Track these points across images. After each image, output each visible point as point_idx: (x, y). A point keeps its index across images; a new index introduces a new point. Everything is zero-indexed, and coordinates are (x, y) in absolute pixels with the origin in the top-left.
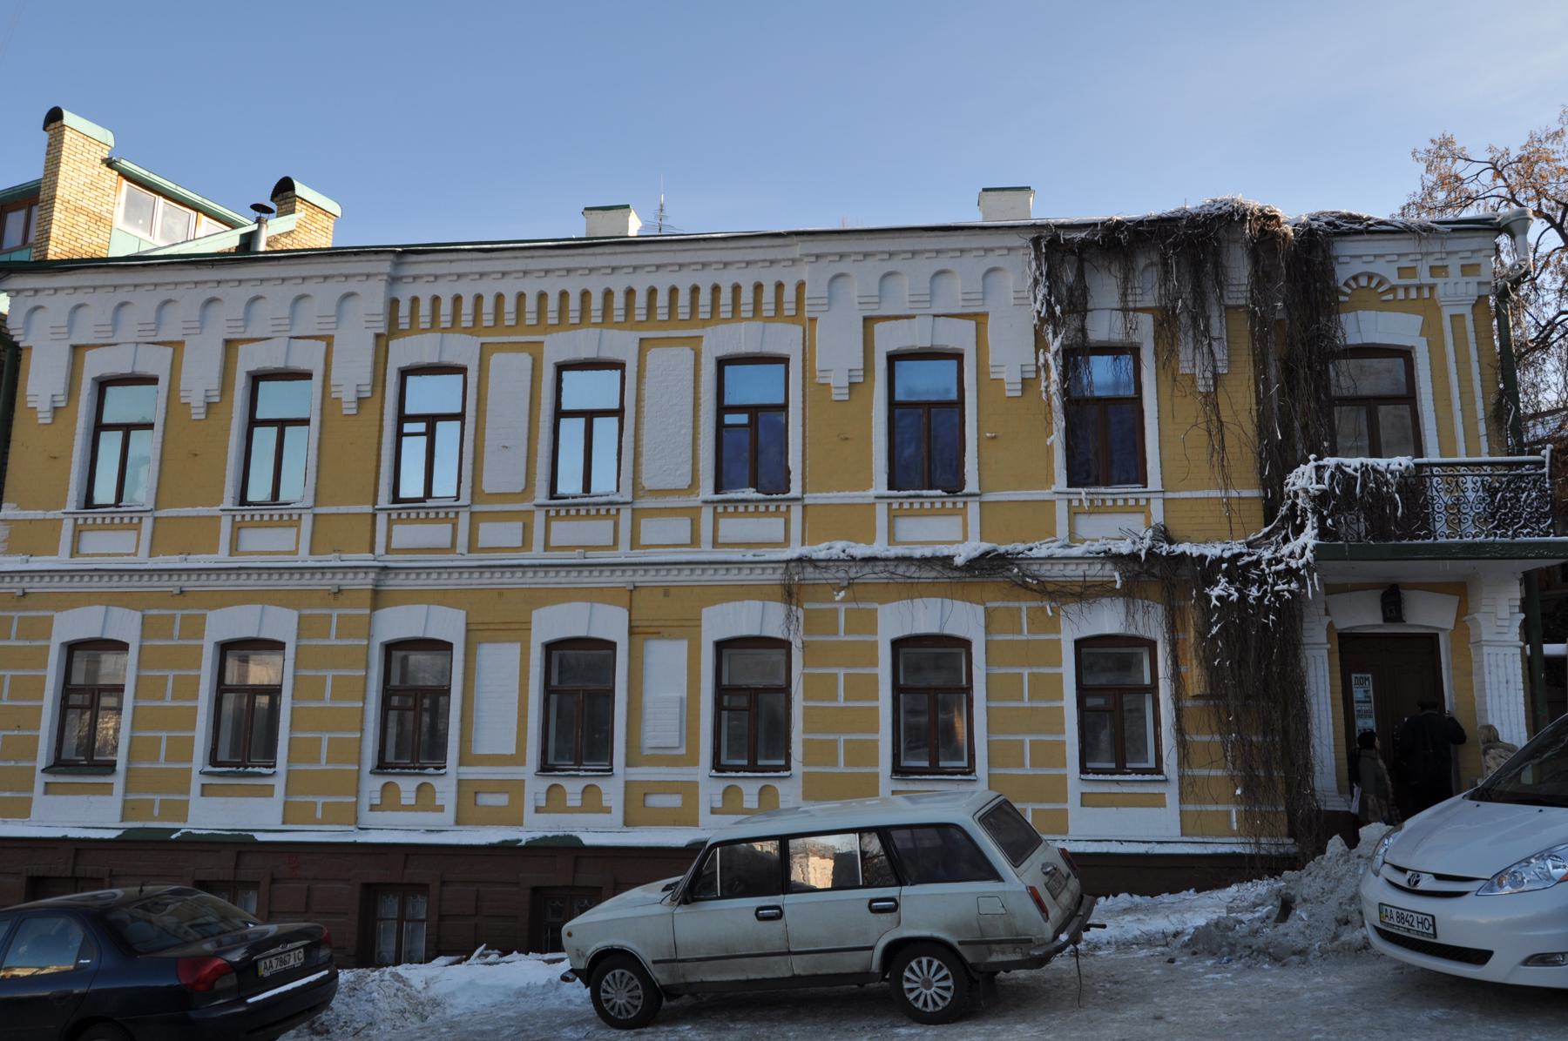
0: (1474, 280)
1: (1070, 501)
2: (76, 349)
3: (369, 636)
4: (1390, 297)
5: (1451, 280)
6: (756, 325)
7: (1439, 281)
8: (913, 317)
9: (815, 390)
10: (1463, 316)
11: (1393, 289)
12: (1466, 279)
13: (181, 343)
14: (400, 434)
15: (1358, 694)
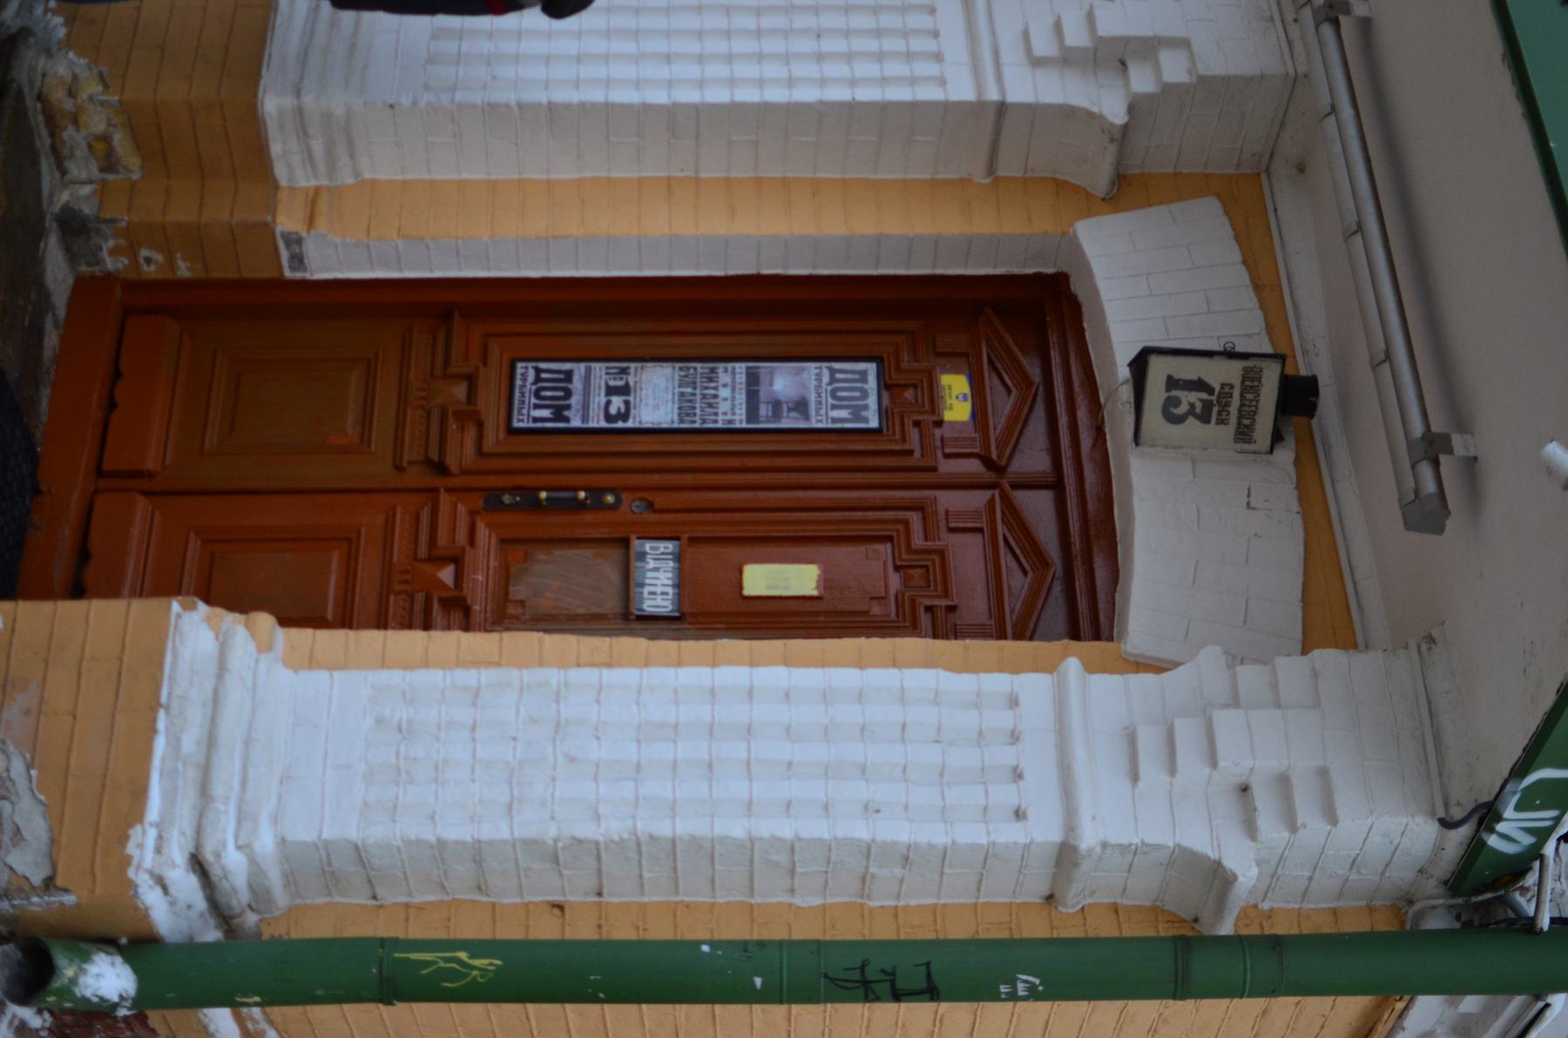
15: (783, 380)
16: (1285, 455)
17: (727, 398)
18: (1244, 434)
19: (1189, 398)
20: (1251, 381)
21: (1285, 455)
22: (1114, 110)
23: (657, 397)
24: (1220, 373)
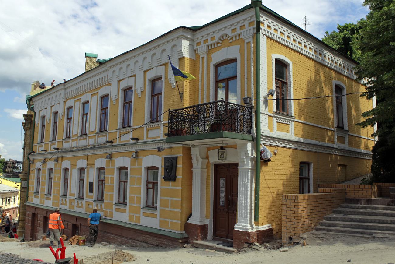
0: (252, 27)
1: (147, 126)
2: (40, 111)
3: (61, 167)
4: (231, 41)
5: (245, 30)
6: (104, 87)
7: (242, 31)
8: (124, 79)
9: (112, 101)
10: (250, 42)
11: (232, 38)
12: (250, 28)
13: (46, 108)
14: (67, 123)
15: (222, 185)
16: (226, 149)
17: (223, 189)
18: (224, 152)
19: (222, 156)
20: (220, 152)
21: (226, 149)
22: (202, 159)
23: (222, 195)
24: (220, 154)
